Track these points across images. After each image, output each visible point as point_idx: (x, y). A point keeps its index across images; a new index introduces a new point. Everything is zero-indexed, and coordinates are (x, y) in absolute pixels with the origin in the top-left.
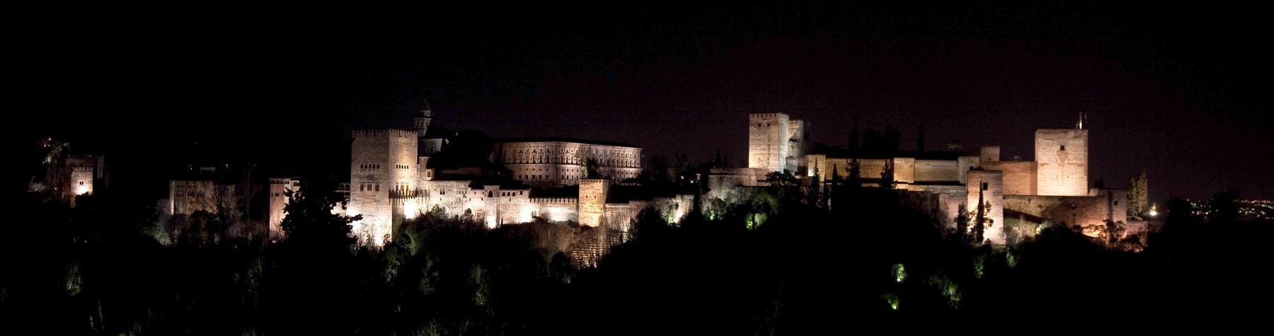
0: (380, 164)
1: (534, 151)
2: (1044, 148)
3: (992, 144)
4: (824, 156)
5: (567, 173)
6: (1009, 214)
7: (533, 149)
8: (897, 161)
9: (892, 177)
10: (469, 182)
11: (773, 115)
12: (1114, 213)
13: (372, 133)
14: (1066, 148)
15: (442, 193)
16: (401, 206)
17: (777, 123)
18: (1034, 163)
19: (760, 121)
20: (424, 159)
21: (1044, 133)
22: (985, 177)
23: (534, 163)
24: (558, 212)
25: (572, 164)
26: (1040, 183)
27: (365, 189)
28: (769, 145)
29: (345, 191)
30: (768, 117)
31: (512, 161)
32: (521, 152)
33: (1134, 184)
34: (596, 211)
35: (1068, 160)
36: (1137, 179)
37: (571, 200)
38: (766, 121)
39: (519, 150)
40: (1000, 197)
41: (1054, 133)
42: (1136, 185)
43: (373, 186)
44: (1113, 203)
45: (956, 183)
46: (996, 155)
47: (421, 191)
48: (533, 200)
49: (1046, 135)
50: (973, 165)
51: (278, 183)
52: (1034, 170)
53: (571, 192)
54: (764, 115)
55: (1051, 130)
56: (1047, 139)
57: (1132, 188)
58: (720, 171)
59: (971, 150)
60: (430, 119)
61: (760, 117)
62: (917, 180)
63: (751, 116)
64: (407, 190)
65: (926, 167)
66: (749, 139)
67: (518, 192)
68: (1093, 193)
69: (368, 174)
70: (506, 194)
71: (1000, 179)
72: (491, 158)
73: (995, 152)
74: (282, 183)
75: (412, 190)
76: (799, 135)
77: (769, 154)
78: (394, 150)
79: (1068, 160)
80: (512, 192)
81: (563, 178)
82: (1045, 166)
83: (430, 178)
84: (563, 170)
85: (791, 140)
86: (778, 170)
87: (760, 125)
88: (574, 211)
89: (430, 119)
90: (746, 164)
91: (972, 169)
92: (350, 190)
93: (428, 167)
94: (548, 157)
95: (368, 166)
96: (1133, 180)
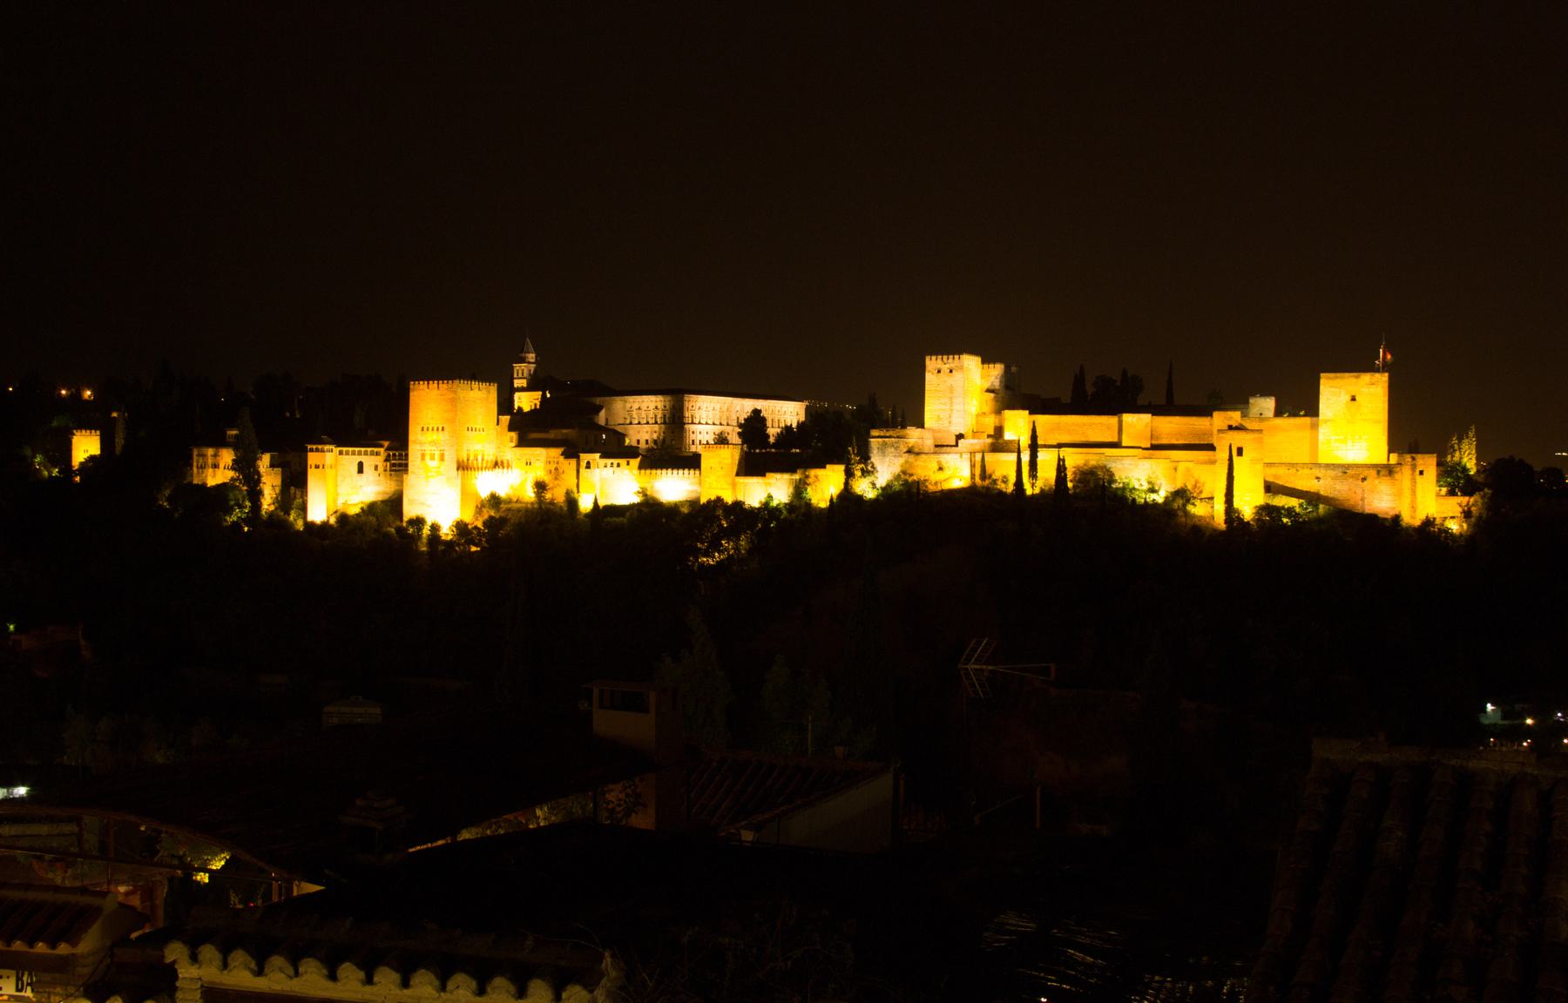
0: (445, 426)
1: (656, 408)
2: (1328, 399)
3: (1265, 394)
4: (1027, 412)
5: (699, 437)
6: (1269, 488)
7: (652, 406)
8: (1128, 418)
9: (1037, 443)
10: (562, 449)
11: (956, 357)
12: (1419, 487)
13: (436, 385)
14: (1357, 398)
15: (528, 463)
16: (474, 481)
17: (961, 368)
18: (1315, 419)
19: (939, 366)
20: (506, 419)
21: (1329, 378)
22: (1237, 439)
23: (656, 423)
24: (673, 487)
25: (707, 424)
26: (1321, 447)
27: (427, 458)
28: (951, 398)
29: (404, 462)
30: (951, 360)
31: (628, 422)
32: (639, 408)
33: (1456, 446)
34: (724, 487)
35: (1361, 414)
36: (1460, 440)
37: (692, 471)
38: (947, 366)
39: (636, 406)
40: (1259, 467)
41: (1341, 378)
42: (1460, 449)
43: (437, 454)
44: (1418, 472)
45: (1211, 447)
46: (1268, 409)
47: (502, 462)
48: (643, 471)
49: (1331, 381)
50: (1231, 423)
51: (317, 450)
52: (1315, 427)
53: (693, 462)
54: (945, 357)
55: (1338, 375)
56: (1332, 387)
57: (1455, 451)
58: (882, 434)
59: (1239, 401)
60: (534, 365)
61: (939, 361)
62: (1154, 442)
63: (928, 358)
64: (483, 460)
65: (1169, 425)
66: (924, 390)
67: (623, 462)
68: (1394, 458)
69: (430, 439)
70: (609, 465)
71: (1260, 441)
72: (602, 418)
73: (1267, 404)
74: (323, 451)
75: (489, 460)
76: (997, 384)
77: (952, 410)
78: (463, 408)
79: (1361, 414)
80: (615, 461)
81: (693, 444)
82: (1328, 423)
83: (514, 444)
84: (693, 433)
85: (988, 391)
86: (962, 432)
87: (939, 372)
88: (696, 487)
89: (534, 365)
90: (920, 424)
91: (1230, 428)
92: (407, 460)
93: (511, 428)
94: (674, 416)
95: (430, 429)
96: (1455, 441)
